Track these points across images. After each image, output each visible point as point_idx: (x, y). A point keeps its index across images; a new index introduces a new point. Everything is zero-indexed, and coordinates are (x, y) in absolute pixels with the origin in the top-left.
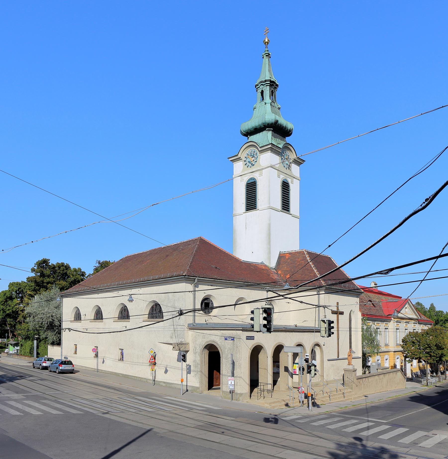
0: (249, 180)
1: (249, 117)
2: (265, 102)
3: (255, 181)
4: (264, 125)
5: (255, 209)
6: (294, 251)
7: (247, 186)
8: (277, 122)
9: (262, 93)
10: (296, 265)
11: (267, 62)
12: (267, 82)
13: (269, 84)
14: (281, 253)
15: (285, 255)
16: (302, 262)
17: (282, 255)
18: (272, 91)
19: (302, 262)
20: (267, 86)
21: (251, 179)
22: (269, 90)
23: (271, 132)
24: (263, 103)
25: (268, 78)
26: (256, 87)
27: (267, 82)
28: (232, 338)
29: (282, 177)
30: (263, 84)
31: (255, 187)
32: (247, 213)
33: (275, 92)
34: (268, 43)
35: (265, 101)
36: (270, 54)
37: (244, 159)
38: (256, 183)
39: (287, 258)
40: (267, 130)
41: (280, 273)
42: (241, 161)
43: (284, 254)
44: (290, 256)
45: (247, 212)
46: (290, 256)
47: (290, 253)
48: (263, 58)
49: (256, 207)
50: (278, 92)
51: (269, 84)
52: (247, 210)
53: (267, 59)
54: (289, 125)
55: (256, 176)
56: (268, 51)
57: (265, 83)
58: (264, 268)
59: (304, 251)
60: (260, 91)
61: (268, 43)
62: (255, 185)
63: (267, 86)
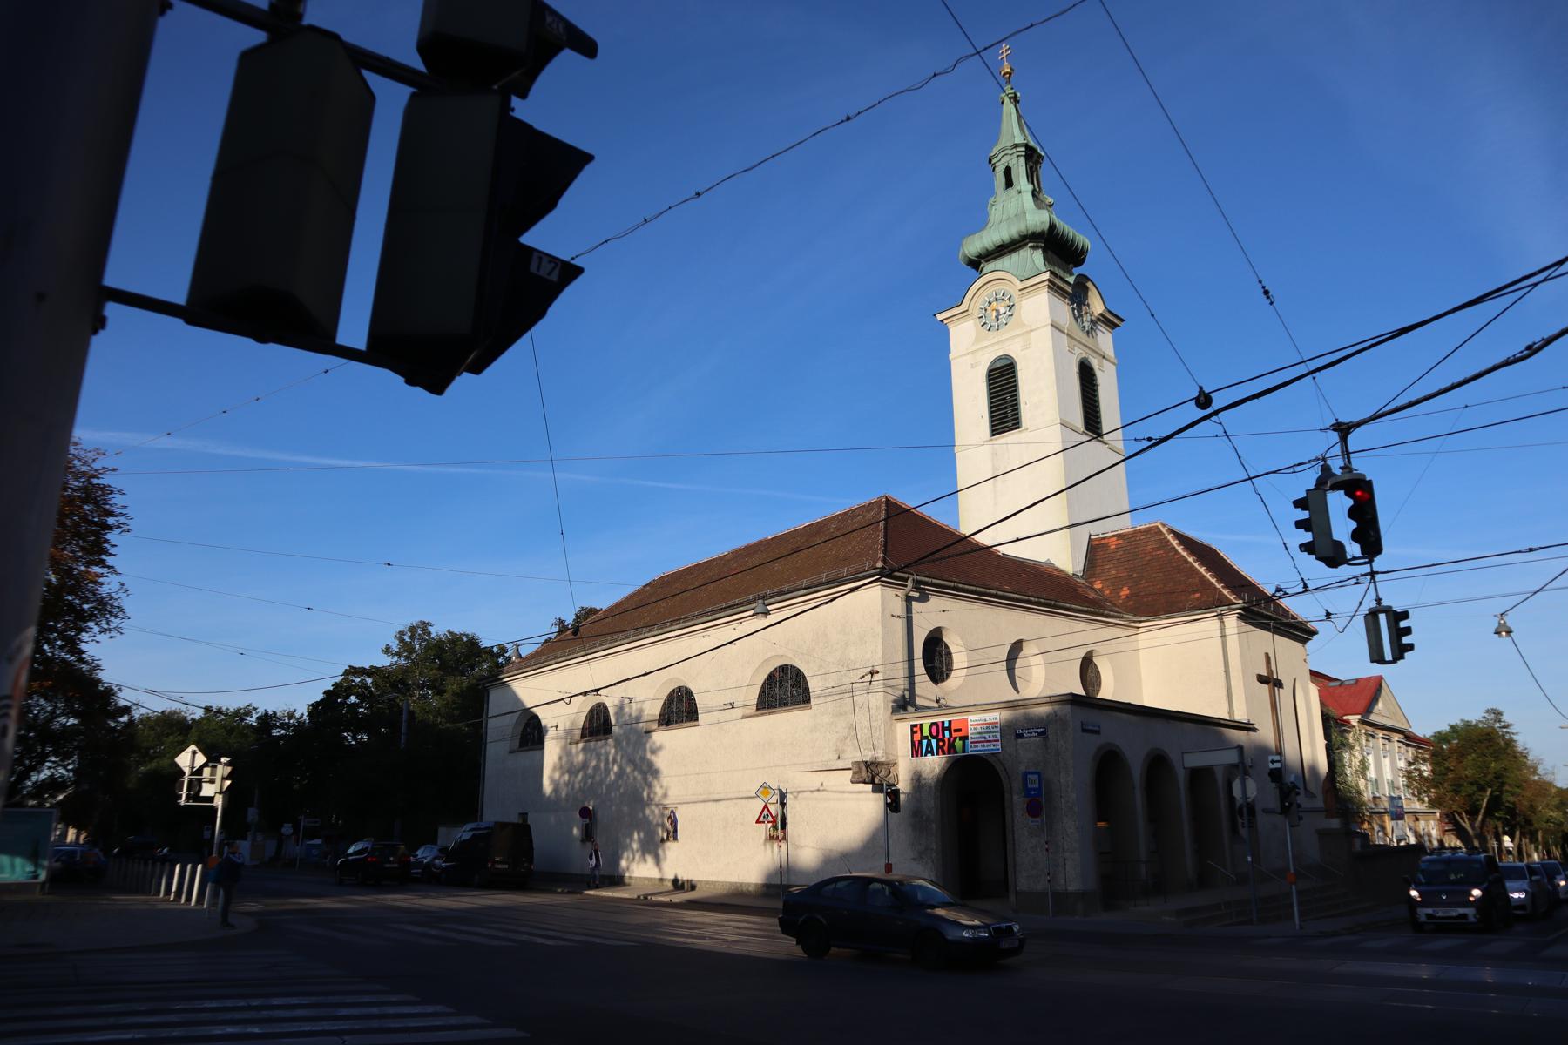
1: (982, 223)
2: (1019, 188)
3: (1009, 362)
4: (1020, 236)
5: (1018, 428)
6: (1129, 530)
7: (989, 376)
8: (1052, 227)
9: (1008, 171)
10: (1144, 563)
11: (1014, 110)
12: (1018, 149)
13: (1023, 154)
14: (1092, 537)
15: (1106, 541)
16: (1159, 552)
17: (1097, 543)
18: (1031, 168)
19: (1159, 552)
20: (1018, 156)
21: (1000, 358)
22: (1024, 165)
23: (1040, 251)
24: (1012, 191)
25: (1019, 139)
26: (990, 162)
27: (1018, 149)
28: (1039, 730)
29: (1080, 353)
30: (1010, 152)
31: (1014, 377)
32: (995, 442)
33: (1036, 169)
34: (1010, 74)
35: (1016, 187)
36: (1019, 94)
37: (977, 313)
38: (1014, 368)
39: (1113, 547)
40: (1031, 247)
41: (1100, 586)
43: (1104, 538)
44: (1120, 542)
45: (996, 439)
46: (1120, 542)
47: (1119, 536)
48: (1002, 103)
49: (1018, 423)
50: (1044, 170)
51: (1023, 154)
52: (994, 435)
53: (1012, 106)
54: (1083, 240)
55: (1014, 350)
56: (1012, 89)
57: (1014, 150)
58: (1056, 573)
59: (1160, 526)
60: (1000, 169)
61: (1010, 74)
62: (1014, 372)
63: (1018, 156)
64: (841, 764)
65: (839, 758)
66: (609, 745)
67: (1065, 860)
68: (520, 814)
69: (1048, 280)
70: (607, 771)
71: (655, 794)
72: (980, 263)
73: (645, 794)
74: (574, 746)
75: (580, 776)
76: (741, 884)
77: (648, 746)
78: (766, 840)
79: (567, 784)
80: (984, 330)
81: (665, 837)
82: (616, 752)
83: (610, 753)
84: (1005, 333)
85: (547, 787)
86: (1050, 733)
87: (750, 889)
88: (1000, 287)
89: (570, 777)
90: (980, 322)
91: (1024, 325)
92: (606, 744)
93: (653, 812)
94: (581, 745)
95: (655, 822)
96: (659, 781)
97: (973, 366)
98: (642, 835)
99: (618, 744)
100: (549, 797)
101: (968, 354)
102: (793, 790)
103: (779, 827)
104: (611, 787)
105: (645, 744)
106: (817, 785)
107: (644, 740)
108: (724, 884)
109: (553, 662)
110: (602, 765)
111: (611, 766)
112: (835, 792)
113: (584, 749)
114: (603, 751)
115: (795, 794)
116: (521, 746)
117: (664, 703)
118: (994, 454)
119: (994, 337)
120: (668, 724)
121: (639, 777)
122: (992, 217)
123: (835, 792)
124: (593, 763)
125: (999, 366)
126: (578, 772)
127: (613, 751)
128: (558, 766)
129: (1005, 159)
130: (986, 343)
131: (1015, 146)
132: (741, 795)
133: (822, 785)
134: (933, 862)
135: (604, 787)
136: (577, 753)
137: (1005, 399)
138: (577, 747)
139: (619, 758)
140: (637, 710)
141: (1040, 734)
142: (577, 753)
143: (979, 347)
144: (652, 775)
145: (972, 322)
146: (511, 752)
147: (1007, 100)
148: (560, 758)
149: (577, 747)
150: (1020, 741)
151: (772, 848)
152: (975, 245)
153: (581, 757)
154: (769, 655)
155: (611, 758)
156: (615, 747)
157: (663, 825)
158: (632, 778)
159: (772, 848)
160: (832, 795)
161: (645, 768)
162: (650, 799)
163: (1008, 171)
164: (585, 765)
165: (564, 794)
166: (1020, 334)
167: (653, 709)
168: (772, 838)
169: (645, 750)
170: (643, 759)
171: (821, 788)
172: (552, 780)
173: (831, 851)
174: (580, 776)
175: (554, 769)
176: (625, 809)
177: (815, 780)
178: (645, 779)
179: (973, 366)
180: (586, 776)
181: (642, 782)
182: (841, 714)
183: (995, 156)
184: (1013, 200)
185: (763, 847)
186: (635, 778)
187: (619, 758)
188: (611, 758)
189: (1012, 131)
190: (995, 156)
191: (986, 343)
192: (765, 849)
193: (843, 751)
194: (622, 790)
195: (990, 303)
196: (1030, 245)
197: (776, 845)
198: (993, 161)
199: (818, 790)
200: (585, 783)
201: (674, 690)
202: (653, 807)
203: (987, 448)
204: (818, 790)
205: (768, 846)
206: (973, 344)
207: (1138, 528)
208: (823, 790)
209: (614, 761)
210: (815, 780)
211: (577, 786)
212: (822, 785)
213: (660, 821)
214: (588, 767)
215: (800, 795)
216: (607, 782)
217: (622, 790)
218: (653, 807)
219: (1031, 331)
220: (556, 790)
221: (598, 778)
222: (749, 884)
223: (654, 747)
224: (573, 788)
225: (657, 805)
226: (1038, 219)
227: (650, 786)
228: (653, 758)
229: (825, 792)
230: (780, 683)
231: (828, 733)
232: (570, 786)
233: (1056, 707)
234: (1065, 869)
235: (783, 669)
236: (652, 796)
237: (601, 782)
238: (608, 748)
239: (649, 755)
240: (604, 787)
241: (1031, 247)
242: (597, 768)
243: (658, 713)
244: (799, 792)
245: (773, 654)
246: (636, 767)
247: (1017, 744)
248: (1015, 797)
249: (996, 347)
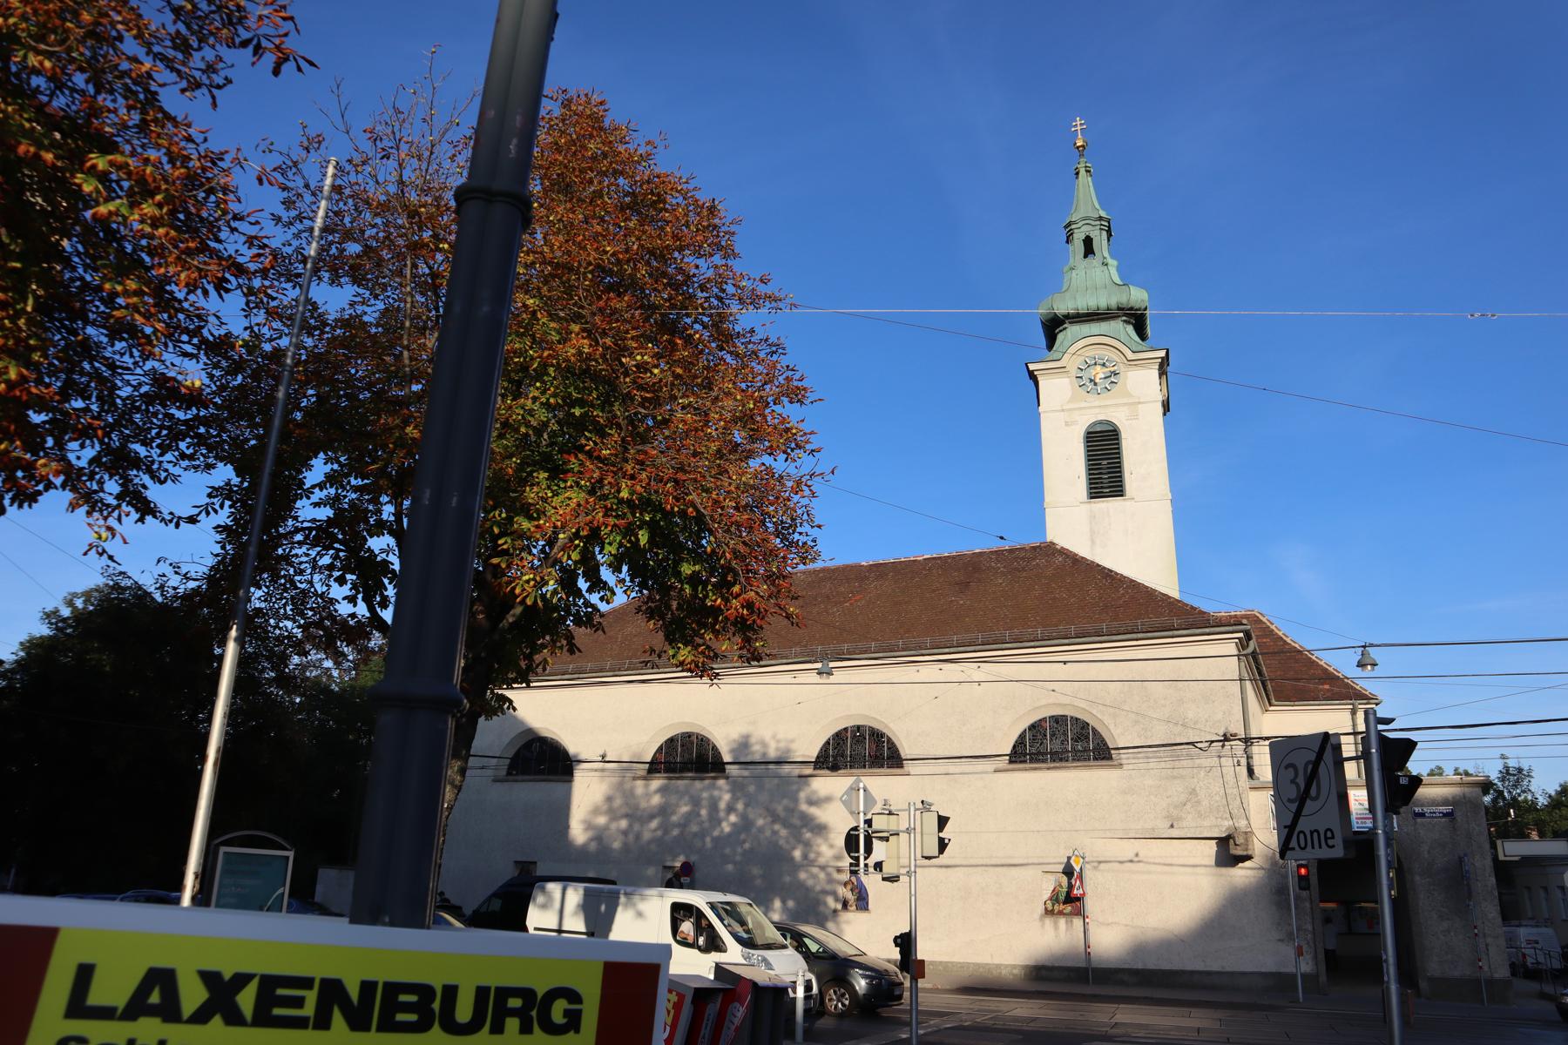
0: (1095, 424)
1: (1057, 288)
3: (1111, 428)
5: (1122, 496)
9: (1088, 242)
11: (1091, 184)
12: (1103, 223)
21: (1100, 422)
24: (1094, 261)
27: (1103, 223)
32: (1093, 505)
37: (1074, 372)
42: (1065, 375)
48: (1077, 174)
49: (1122, 491)
52: (1092, 498)
53: (1090, 179)
55: (1119, 418)
57: (1098, 223)
60: (1079, 237)
61: (1083, 146)
64: (1175, 833)
65: (1172, 826)
66: (720, 789)
67: (1487, 945)
68: (516, 862)
69: (1162, 358)
70: (715, 820)
71: (819, 854)
72: (1063, 323)
73: (797, 854)
74: (640, 783)
75: (654, 824)
76: (998, 966)
77: (802, 795)
78: (1042, 918)
79: (625, 833)
80: (1082, 391)
81: (839, 906)
82: (735, 799)
83: (720, 798)
84: (1106, 399)
85: (578, 832)
86: (1458, 815)
87: (1004, 972)
88: (1107, 354)
89: (630, 826)
90: (1076, 383)
91: (1130, 395)
92: (713, 787)
93: (815, 877)
94: (656, 784)
95: (818, 888)
96: (826, 839)
97: (1067, 424)
98: (791, 904)
99: (737, 787)
100: (584, 846)
101: (1063, 410)
102: (1091, 859)
103: (1068, 901)
104: (720, 841)
105: (798, 790)
106: (1131, 855)
107: (794, 787)
108: (963, 965)
109: (611, 674)
110: (704, 812)
111: (722, 814)
112: (1159, 864)
113: (662, 790)
114: (705, 795)
115: (1096, 864)
116: (509, 774)
117: (828, 743)
118: (1092, 518)
119: (1093, 400)
120: (835, 768)
121: (784, 832)
122: (1073, 281)
123: (1159, 864)
124: (685, 809)
125: (1099, 429)
126: (652, 817)
127: (727, 797)
128: (605, 807)
129: (1083, 229)
130: (1083, 404)
131: (1101, 218)
132: (994, 862)
133: (1137, 855)
134: (1308, 943)
135: (708, 840)
136: (648, 795)
137: (1100, 464)
138: (646, 786)
139: (740, 806)
140: (777, 749)
141: (1445, 815)
142: (648, 795)
143: (1071, 406)
144: (812, 830)
145: (1066, 380)
146: (496, 781)
147: (1082, 172)
148: (609, 799)
149: (646, 786)
150: (1419, 820)
151: (1056, 924)
152: (1063, 307)
153: (656, 800)
154: (1043, 702)
155: (722, 805)
156: (733, 791)
157: (834, 894)
158: (768, 833)
159: (1056, 924)
160: (1153, 868)
161: (796, 821)
162: (808, 861)
163: (1088, 242)
164: (663, 811)
165: (616, 845)
166: (1125, 404)
167: (809, 749)
168: (1049, 912)
169: (796, 800)
170: (791, 811)
171: (1136, 859)
172: (589, 826)
173: (1155, 929)
174: (654, 824)
175: (596, 811)
176: (756, 871)
177: (1127, 849)
178: (799, 839)
179: (1067, 424)
180: (665, 828)
181: (792, 840)
182: (1175, 778)
183: (1075, 223)
184: (1097, 270)
185: (1038, 924)
186: (775, 833)
187: (740, 806)
188: (722, 805)
189: (1087, 200)
190: (1075, 223)
191: (1083, 404)
192: (1043, 926)
193: (1179, 819)
194: (747, 846)
195: (1095, 364)
196: (1124, 318)
197: (1062, 921)
198: (1073, 227)
199: (1131, 861)
200: (666, 832)
201: (846, 729)
202: (815, 870)
203: (1087, 506)
204: (1131, 861)
205: (1048, 921)
206: (1070, 401)
207: (1233, 613)
208: (1139, 862)
209: (730, 809)
210: (1127, 849)
211: (647, 836)
212: (1137, 855)
213: (828, 887)
214: (673, 813)
215: (1102, 865)
216: (716, 833)
217: (747, 846)
218: (815, 870)
219: (1139, 403)
220: (599, 836)
221: (694, 828)
222: (1014, 967)
223: (814, 798)
224: (638, 836)
225: (823, 868)
226: (1137, 296)
227: (807, 845)
228: (813, 811)
229: (1141, 864)
230: (1053, 735)
231: (1152, 797)
232: (631, 837)
233: (1467, 790)
234: (1488, 955)
235: (1058, 720)
236: (812, 856)
237: (702, 834)
238: (716, 793)
239: (804, 807)
240: (708, 840)
241: (1125, 321)
242: (689, 818)
243: (815, 754)
244: (1100, 862)
245: (1051, 701)
246: (776, 818)
247: (1416, 823)
248: (1417, 878)
249: (1097, 411)
